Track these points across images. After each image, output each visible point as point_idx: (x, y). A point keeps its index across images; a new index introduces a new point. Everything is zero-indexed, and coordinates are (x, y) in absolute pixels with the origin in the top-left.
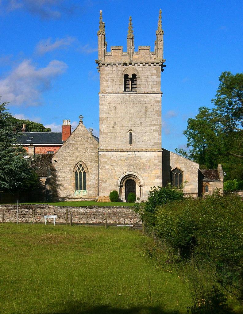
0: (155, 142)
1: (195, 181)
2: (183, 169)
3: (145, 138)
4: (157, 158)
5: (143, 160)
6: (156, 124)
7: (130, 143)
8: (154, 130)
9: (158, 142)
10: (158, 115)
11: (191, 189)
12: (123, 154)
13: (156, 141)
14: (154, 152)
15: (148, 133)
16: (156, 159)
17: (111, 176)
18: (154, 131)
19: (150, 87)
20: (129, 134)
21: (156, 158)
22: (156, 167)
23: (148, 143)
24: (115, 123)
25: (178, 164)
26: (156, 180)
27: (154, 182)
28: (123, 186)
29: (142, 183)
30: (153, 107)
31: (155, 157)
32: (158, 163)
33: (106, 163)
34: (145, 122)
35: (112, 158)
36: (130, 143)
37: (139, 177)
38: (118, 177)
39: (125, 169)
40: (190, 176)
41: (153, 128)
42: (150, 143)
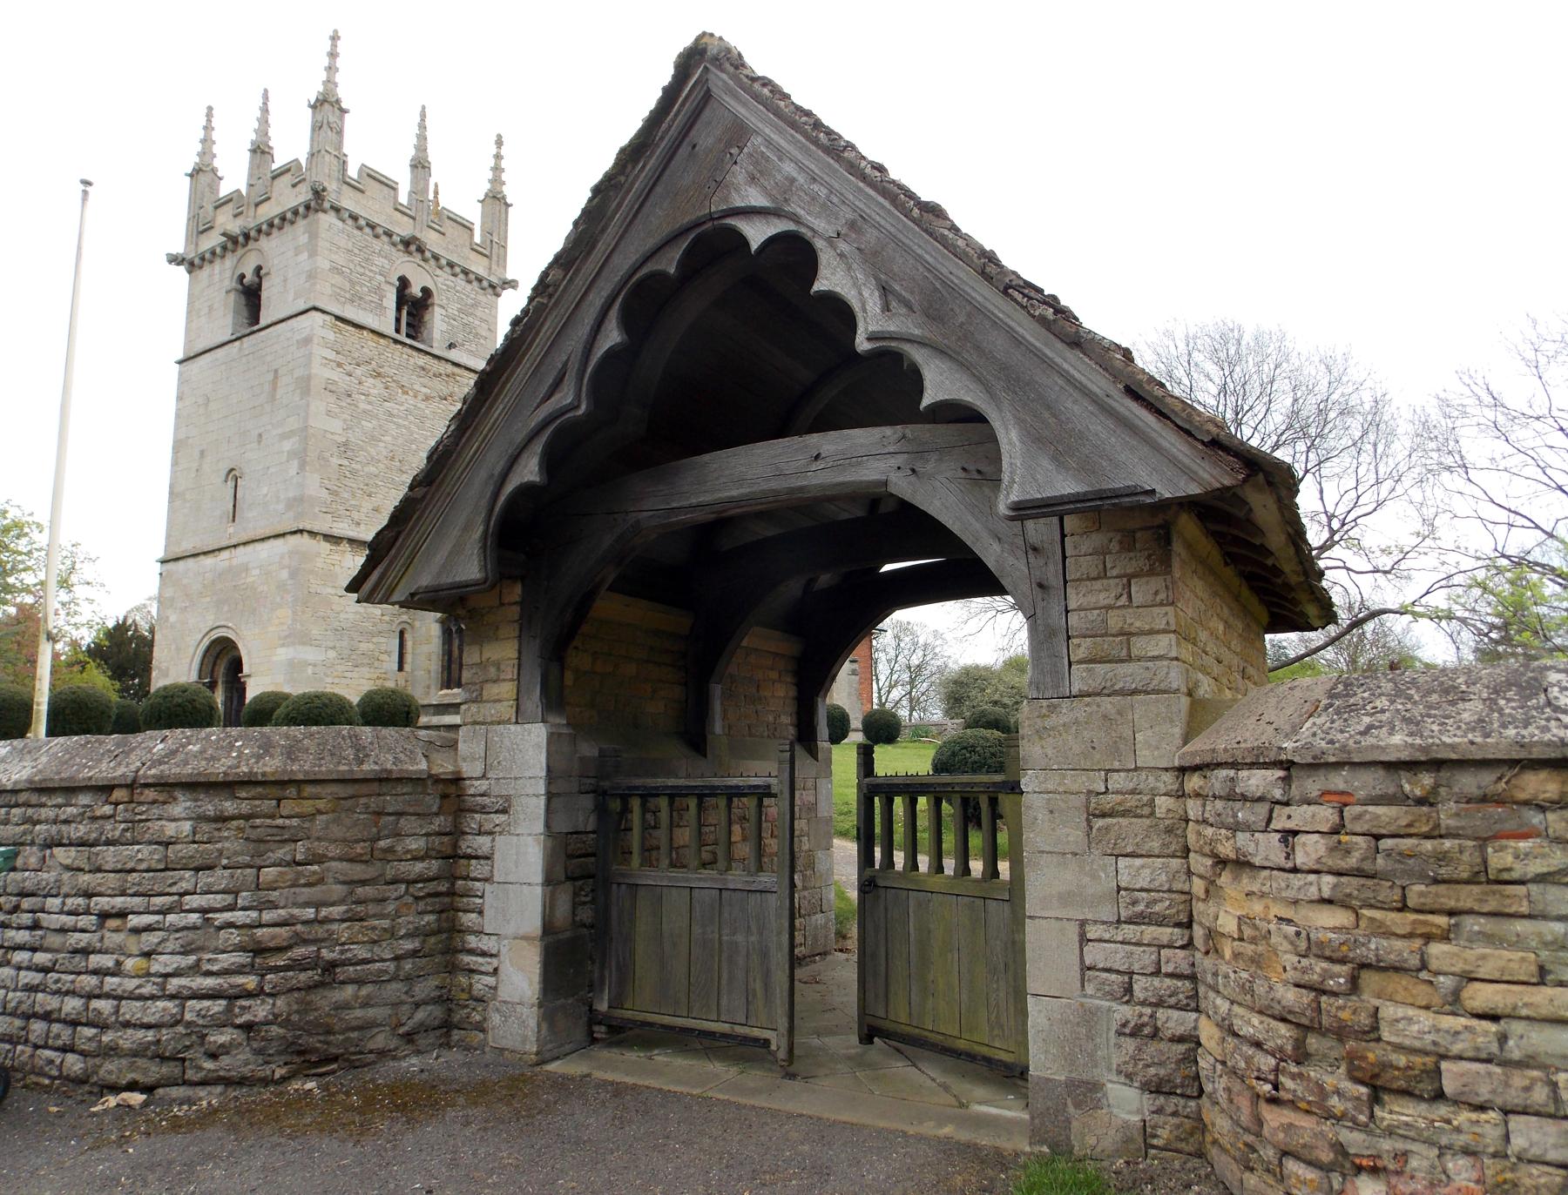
3: (265, 490)
5: (254, 576)
9: (295, 499)
12: (208, 561)
14: (280, 541)
17: (178, 649)
18: (292, 454)
24: (202, 453)
35: (185, 581)
38: (191, 650)
41: (287, 445)
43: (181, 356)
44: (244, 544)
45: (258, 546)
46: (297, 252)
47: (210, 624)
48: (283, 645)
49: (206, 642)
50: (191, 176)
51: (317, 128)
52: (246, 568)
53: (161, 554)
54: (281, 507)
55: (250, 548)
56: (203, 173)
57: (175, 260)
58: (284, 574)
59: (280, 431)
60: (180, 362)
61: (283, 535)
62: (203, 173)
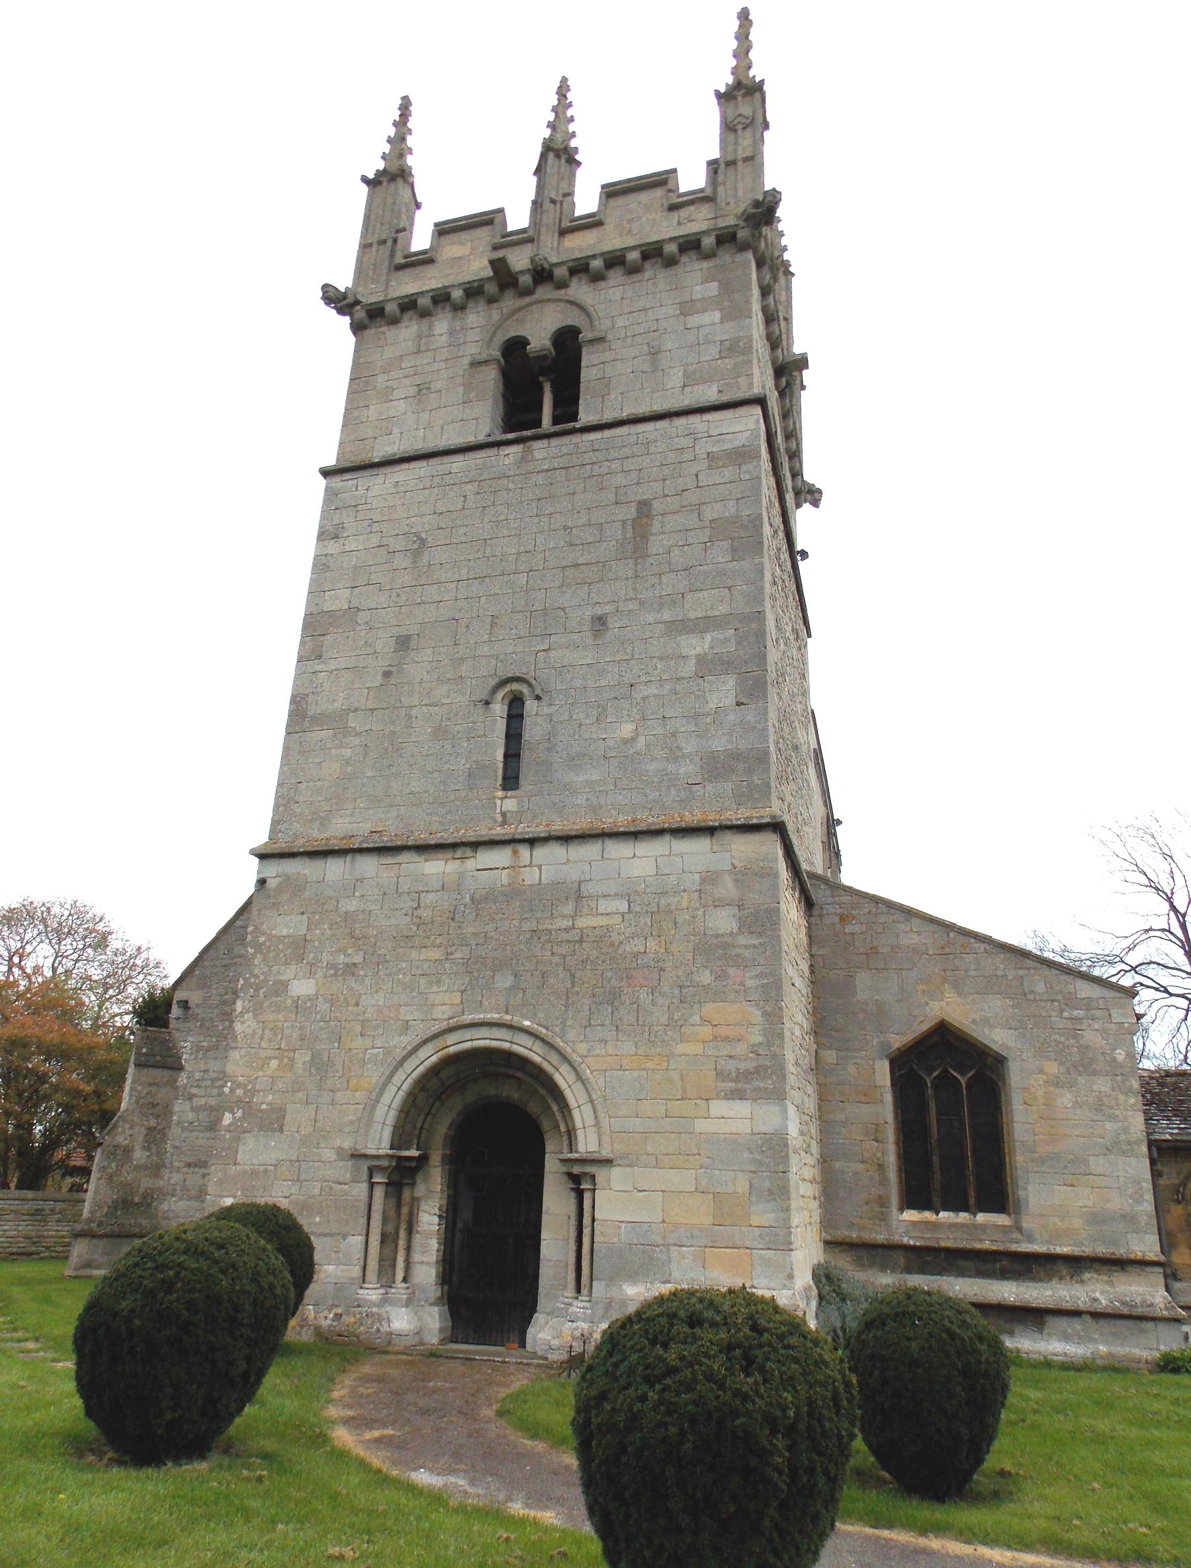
0: (713, 756)
1: (1116, 1143)
2: (997, 1038)
3: (627, 730)
4: (727, 889)
5: (608, 912)
6: (723, 609)
7: (511, 781)
8: (701, 660)
10: (734, 550)
11: (1096, 1218)
12: (435, 867)
13: (719, 744)
14: (700, 845)
15: (652, 690)
16: (719, 904)
17: (320, 1066)
18: (707, 666)
19: (675, 379)
20: (500, 709)
21: (719, 892)
22: (721, 976)
23: (652, 767)
24: (403, 643)
25: (950, 996)
26: (719, 1107)
27: (701, 1125)
28: (423, 1160)
29: (587, 1143)
30: (692, 497)
31: (710, 879)
32: (742, 940)
33: (299, 949)
34: (630, 606)
35: (351, 905)
36: (511, 781)
37: (563, 1079)
38: (373, 1076)
39: (445, 1004)
40: (1065, 1099)
41: (696, 646)
42: (671, 767)
43: (331, 461)
44: (566, 839)
45: (619, 850)
46: (687, 308)
47: (443, 1014)
48: (736, 1095)
49: (429, 1056)
50: (371, 183)
51: (729, 128)
52: (578, 895)
53: (261, 837)
54: (687, 769)
55: (590, 850)
56: (391, 181)
57: (334, 298)
58: (723, 921)
59: (666, 616)
60: (326, 473)
61: (709, 831)
62: (391, 181)
